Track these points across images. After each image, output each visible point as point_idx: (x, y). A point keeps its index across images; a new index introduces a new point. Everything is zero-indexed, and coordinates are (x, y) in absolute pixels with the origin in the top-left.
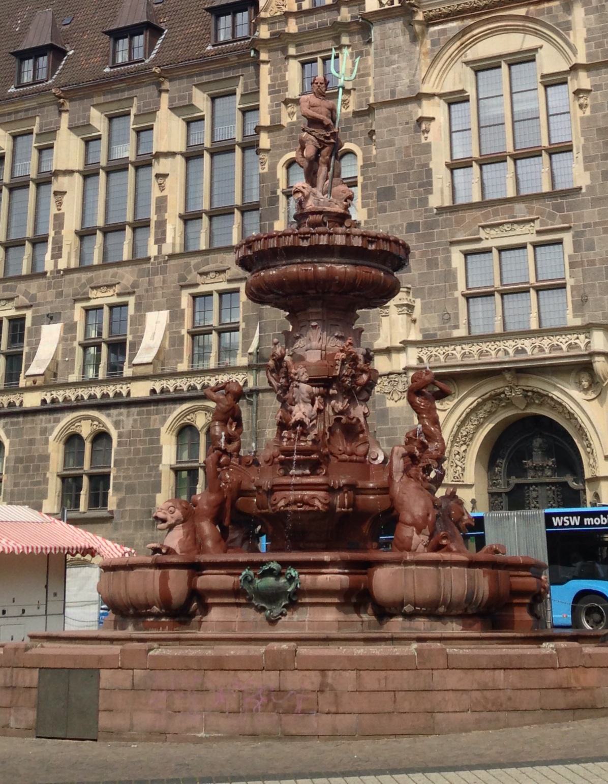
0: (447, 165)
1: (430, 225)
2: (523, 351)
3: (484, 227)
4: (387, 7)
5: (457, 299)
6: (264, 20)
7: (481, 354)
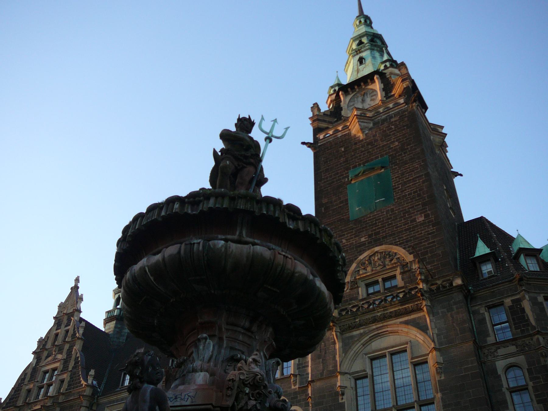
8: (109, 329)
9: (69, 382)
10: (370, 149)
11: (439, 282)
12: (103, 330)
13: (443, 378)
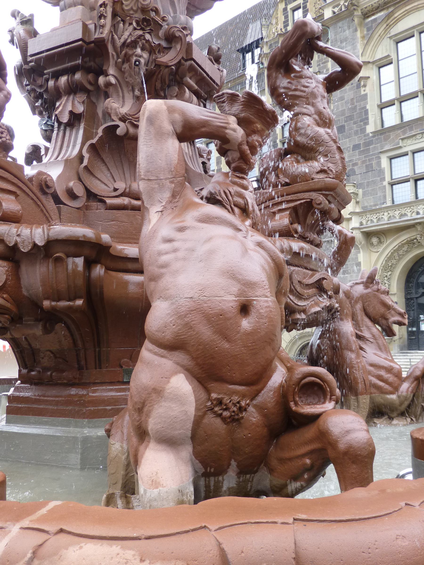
0: (378, 106)
1: (368, 144)
3: (402, 139)
4: (337, 13)
5: (385, 186)
7: (402, 216)
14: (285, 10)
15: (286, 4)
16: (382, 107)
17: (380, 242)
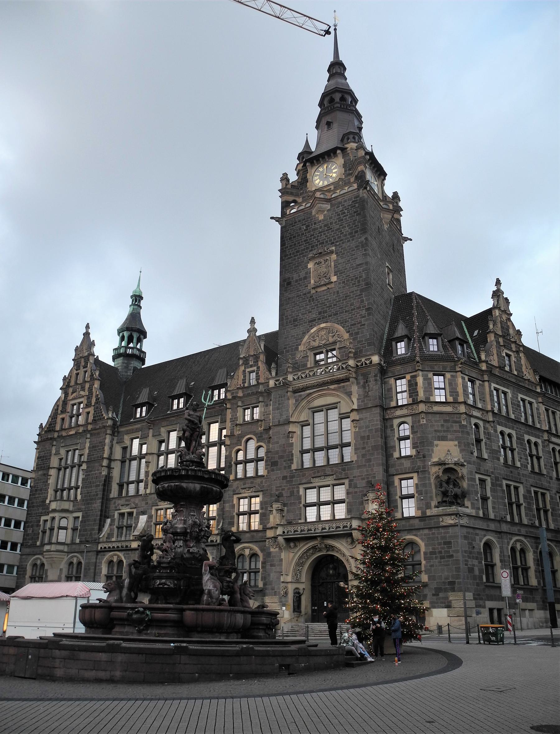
2: (325, 529)
6: (229, 391)
8: (118, 364)
9: (94, 414)
10: (327, 230)
11: (363, 360)
12: (112, 364)
13: (357, 430)
14: (244, 371)
15: (245, 368)
16: (303, 452)
17: (296, 546)
